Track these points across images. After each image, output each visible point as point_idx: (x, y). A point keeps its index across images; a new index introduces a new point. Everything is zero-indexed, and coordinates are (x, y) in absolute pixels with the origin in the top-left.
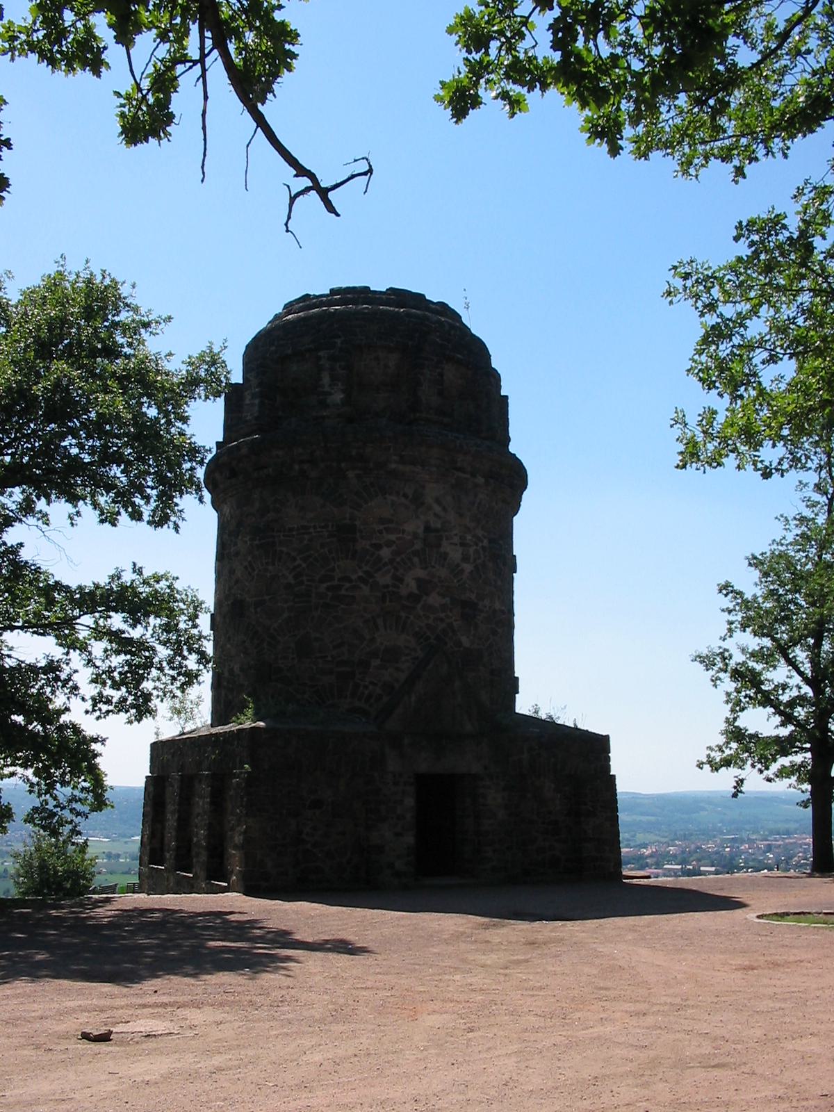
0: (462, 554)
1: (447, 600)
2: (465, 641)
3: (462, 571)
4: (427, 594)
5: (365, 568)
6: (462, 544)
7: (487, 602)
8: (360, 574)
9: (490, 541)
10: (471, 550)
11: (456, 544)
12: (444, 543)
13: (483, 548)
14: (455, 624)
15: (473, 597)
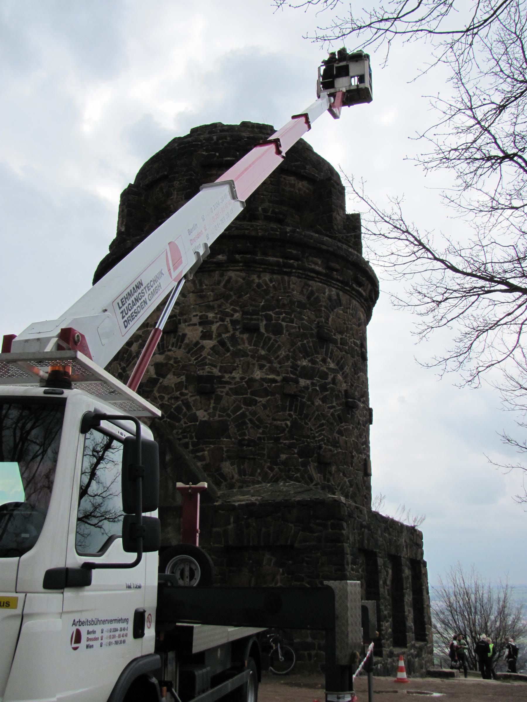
0: (202, 332)
1: (183, 378)
2: (202, 415)
3: (203, 347)
4: (164, 377)
5: (123, 365)
6: (201, 324)
7: (237, 375)
8: (120, 371)
9: (244, 313)
10: (214, 327)
11: (195, 325)
12: (183, 325)
13: (234, 323)
14: (191, 400)
15: (216, 371)
